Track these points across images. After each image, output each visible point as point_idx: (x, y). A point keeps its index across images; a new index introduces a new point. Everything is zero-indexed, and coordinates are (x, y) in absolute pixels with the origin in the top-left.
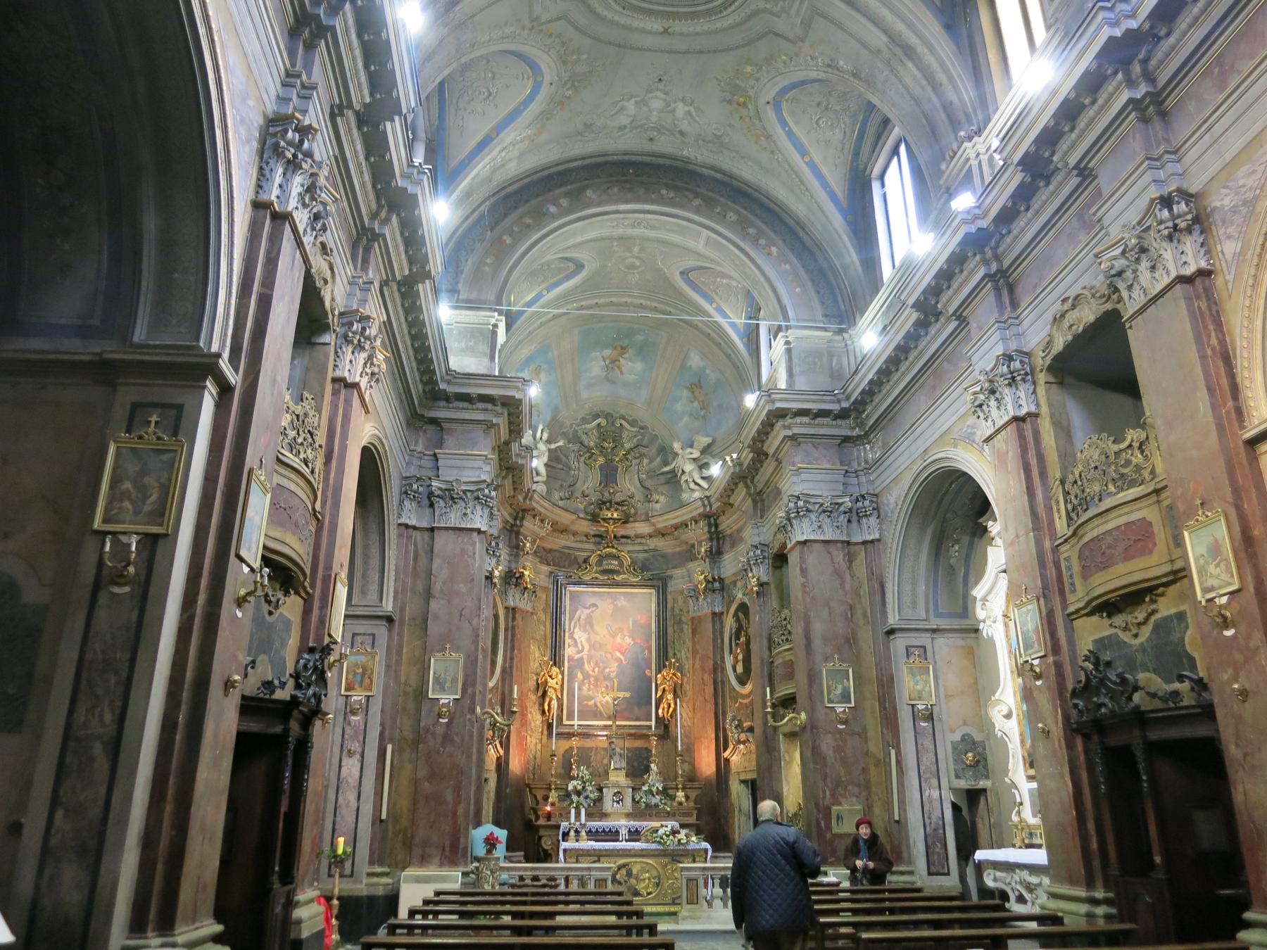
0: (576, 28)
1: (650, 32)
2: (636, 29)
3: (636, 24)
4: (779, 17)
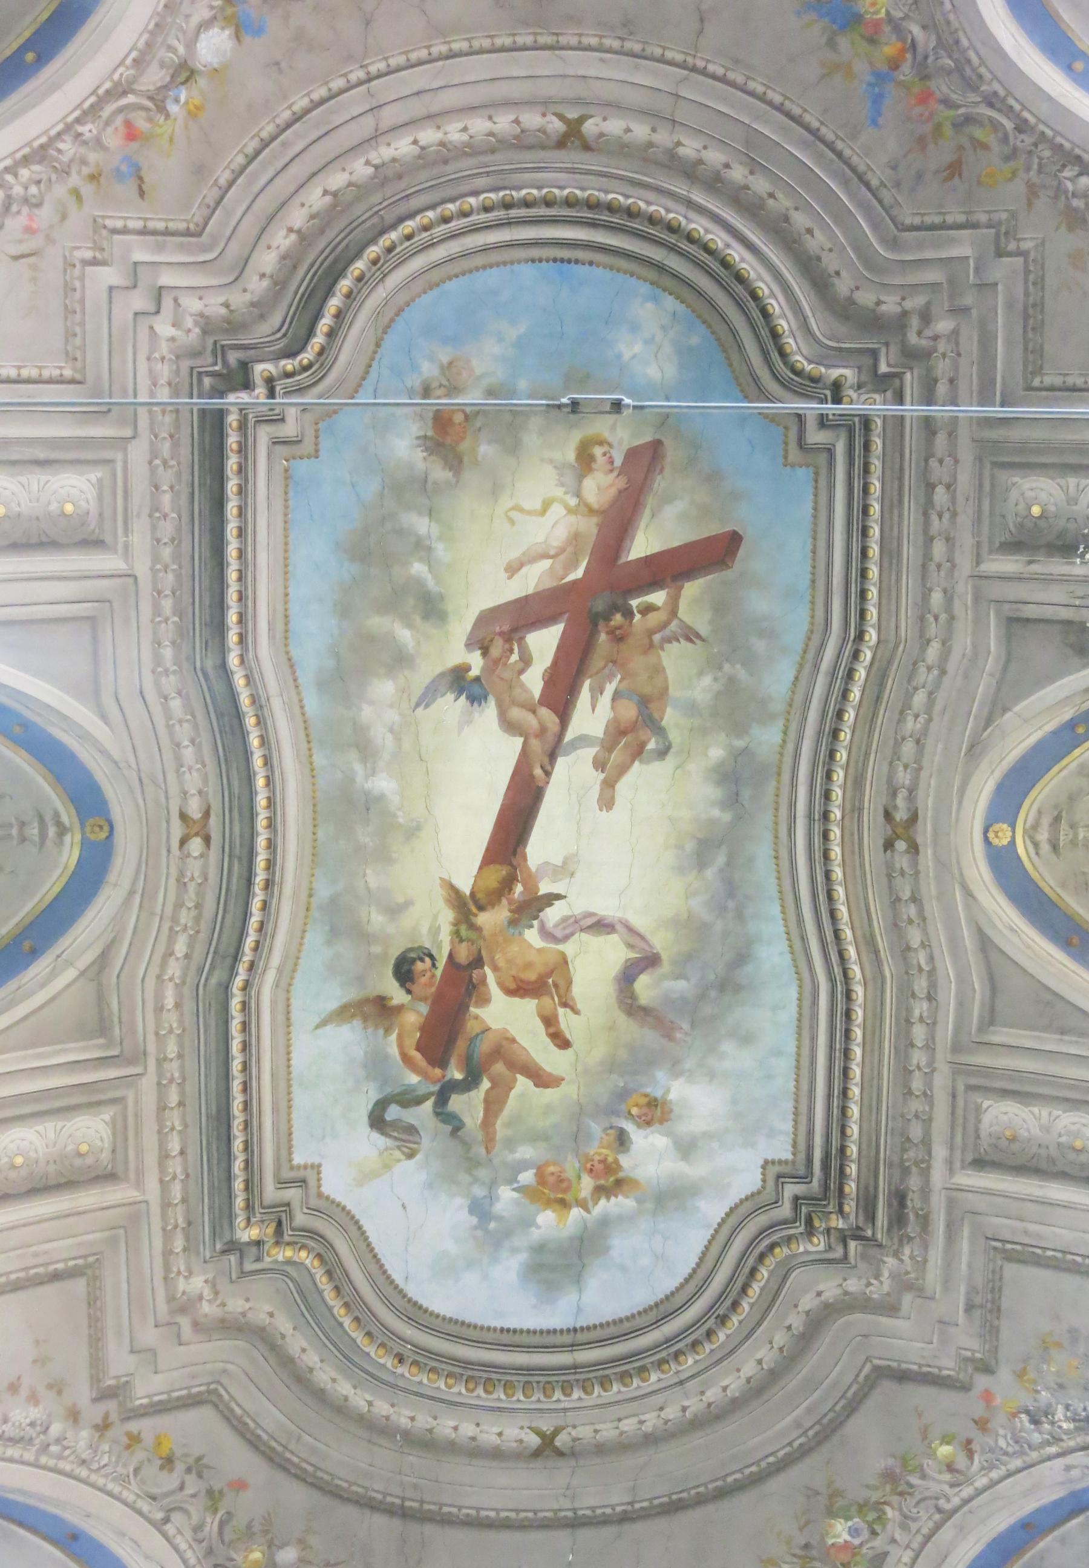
0: (254, 1443)
1: (496, 1454)
2: (452, 1448)
3: (446, 1426)
4: (891, 1309)
